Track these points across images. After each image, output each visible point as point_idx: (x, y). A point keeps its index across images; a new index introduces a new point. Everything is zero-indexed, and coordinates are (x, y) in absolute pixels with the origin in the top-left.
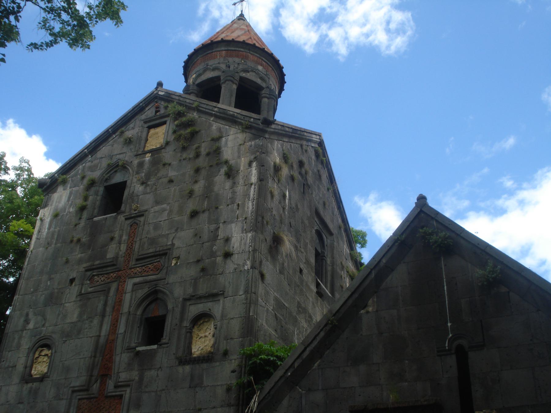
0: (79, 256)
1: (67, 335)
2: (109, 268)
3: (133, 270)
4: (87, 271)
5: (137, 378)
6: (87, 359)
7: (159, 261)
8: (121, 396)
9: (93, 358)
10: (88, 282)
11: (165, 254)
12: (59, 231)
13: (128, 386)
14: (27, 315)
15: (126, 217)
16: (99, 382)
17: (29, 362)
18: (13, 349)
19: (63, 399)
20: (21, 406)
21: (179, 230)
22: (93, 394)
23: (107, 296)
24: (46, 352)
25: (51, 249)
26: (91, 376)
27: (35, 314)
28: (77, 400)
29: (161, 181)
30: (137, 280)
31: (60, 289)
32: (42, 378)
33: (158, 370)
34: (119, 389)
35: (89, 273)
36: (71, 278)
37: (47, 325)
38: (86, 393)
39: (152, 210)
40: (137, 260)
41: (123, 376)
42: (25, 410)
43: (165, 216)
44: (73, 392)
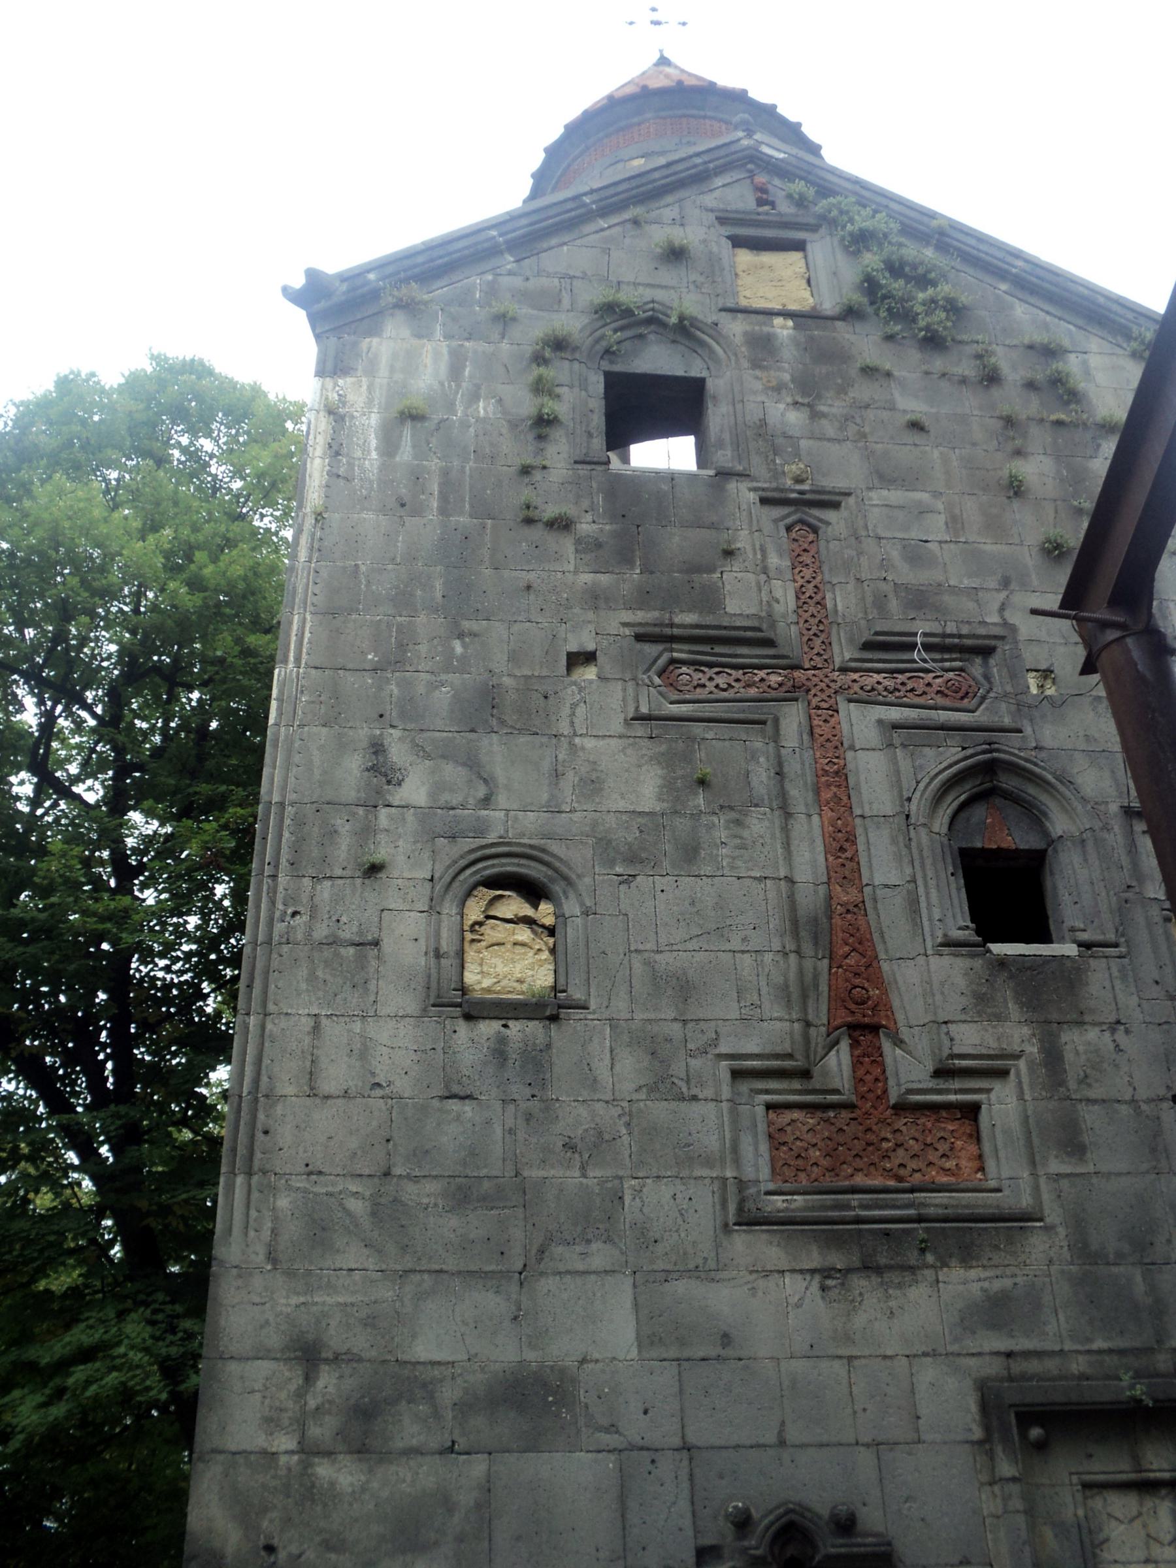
0: (586, 578)
1: (633, 859)
2: (744, 650)
3: (856, 676)
4: (639, 638)
5: (1033, 1049)
6: (768, 957)
7: (962, 670)
8: (971, 1111)
9: (793, 957)
10: (657, 681)
11: (986, 652)
12: (445, 473)
13: (1003, 1074)
14: (377, 748)
15: (764, 494)
16: (845, 1045)
17: (445, 934)
18: (338, 872)
19: (695, 1098)
20: (468, 1108)
21: (1013, 586)
22: (836, 1091)
23: (779, 747)
24: (513, 906)
25: (427, 527)
26: (808, 1024)
27: (421, 751)
28: (760, 1110)
29: (870, 414)
30: (895, 714)
31: (526, 677)
32: (549, 1009)
33: (1113, 1031)
34: (957, 1084)
35: (652, 649)
36: (573, 647)
37: (502, 800)
38: (796, 1085)
39: (876, 497)
40: (868, 646)
41: (971, 1038)
42: (499, 1131)
43: (936, 527)
44: (737, 1075)
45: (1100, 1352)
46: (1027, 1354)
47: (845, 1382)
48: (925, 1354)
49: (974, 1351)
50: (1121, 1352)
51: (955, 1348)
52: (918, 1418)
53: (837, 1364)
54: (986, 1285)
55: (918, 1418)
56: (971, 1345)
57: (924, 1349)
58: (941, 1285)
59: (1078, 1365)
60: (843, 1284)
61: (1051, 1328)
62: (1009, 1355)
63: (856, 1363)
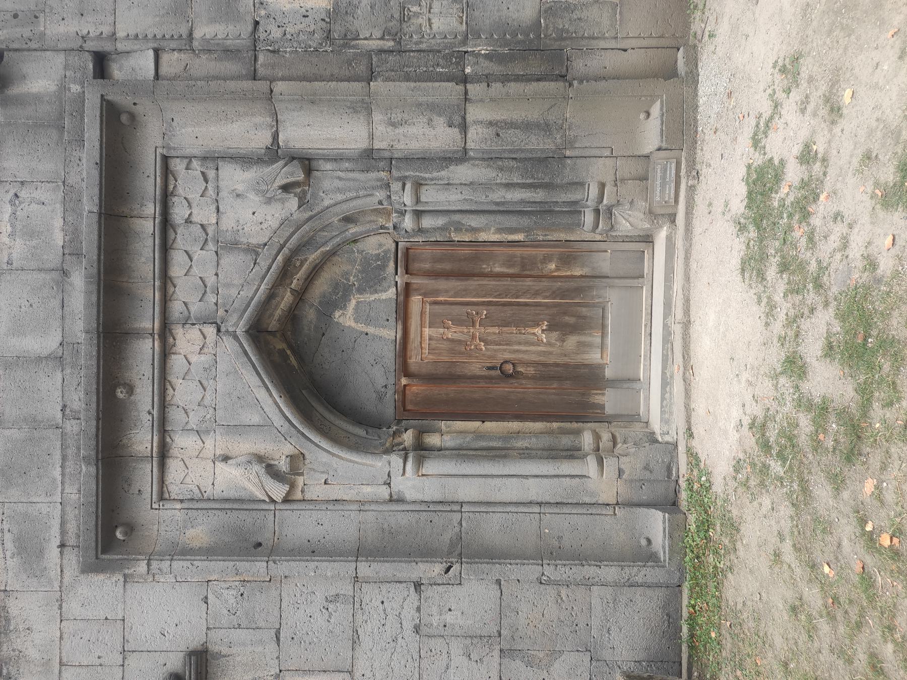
45: (63, 475)
46: (63, 532)
47: (78, 670)
48: (60, 607)
49: (59, 570)
50: (64, 458)
51: (56, 585)
52: (106, 619)
53: (64, 675)
54: (8, 554)
55: (106, 619)
56: (54, 573)
57: (56, 608)
58: (8, 589)
59: (72, 491)
60: (6, 663)
61: (45, 509)
62: (62, 546)
63: (65, 660)
